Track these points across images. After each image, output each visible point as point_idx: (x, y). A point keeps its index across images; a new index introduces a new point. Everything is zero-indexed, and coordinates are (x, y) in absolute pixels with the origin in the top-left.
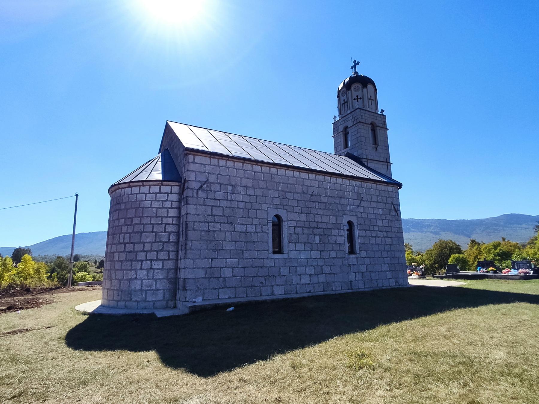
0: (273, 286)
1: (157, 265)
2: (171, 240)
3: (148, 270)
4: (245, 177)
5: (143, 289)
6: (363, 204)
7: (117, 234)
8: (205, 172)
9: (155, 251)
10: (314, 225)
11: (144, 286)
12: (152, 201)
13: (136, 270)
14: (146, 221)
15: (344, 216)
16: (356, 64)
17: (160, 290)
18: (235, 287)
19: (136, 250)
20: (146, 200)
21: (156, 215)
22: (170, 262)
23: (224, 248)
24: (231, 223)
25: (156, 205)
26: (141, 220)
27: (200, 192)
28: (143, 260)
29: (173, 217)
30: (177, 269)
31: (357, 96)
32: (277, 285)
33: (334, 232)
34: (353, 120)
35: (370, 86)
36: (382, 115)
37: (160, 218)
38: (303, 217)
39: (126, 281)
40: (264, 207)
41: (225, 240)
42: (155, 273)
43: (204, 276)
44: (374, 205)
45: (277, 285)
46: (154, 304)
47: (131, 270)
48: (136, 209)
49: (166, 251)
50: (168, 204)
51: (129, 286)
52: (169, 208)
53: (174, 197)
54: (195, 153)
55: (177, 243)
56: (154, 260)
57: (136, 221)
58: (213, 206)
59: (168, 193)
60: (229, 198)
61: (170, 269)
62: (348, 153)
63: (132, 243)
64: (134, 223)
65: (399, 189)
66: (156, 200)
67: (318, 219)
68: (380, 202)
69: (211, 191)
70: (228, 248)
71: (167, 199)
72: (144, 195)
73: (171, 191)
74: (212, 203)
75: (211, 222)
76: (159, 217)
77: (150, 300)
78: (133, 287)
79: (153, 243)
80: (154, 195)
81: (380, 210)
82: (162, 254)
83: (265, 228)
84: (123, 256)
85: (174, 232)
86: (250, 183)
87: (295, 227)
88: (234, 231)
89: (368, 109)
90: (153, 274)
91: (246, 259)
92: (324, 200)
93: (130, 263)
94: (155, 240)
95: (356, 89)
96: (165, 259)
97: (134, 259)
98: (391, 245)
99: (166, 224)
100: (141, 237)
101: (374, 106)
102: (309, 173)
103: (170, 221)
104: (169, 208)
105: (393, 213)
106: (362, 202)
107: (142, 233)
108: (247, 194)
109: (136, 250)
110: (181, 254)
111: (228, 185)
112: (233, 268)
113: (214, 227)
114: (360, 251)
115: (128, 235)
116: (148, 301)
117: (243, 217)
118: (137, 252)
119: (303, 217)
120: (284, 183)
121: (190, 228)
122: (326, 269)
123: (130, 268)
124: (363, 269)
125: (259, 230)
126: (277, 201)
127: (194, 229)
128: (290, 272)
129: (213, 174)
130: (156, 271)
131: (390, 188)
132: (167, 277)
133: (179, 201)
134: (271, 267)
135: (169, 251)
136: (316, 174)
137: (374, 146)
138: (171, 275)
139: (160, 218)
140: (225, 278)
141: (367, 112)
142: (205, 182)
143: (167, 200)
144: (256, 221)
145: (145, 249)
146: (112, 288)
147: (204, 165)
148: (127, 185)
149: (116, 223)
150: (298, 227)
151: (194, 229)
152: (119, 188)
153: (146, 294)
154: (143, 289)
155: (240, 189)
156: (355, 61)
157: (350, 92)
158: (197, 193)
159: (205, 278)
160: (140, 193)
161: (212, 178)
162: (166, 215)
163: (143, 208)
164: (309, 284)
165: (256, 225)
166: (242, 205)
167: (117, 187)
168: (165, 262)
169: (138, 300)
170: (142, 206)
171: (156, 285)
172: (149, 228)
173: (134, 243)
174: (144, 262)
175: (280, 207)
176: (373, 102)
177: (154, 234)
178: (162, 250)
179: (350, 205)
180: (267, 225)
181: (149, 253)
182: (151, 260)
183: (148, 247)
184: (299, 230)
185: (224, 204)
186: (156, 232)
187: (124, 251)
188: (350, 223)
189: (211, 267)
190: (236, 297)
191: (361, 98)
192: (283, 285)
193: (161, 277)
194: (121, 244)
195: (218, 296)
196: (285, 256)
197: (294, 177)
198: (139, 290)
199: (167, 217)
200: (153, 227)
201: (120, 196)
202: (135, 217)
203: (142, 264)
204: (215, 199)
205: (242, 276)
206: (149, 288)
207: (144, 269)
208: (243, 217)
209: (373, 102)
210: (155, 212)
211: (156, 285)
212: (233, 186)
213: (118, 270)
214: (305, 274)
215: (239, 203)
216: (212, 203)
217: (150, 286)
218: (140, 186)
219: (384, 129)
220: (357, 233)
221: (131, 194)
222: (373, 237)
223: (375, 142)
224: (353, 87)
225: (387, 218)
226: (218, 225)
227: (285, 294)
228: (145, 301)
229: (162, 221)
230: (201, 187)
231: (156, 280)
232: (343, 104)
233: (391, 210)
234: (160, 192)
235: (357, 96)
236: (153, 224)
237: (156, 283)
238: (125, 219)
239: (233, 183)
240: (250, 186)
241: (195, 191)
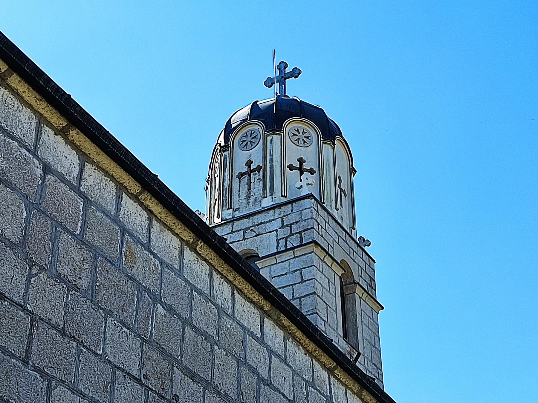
16: (285, 74)
31: (301, 161)
34: (282, 233)
156: (282, 66)
232: (241, 175)
235: (301, 161)
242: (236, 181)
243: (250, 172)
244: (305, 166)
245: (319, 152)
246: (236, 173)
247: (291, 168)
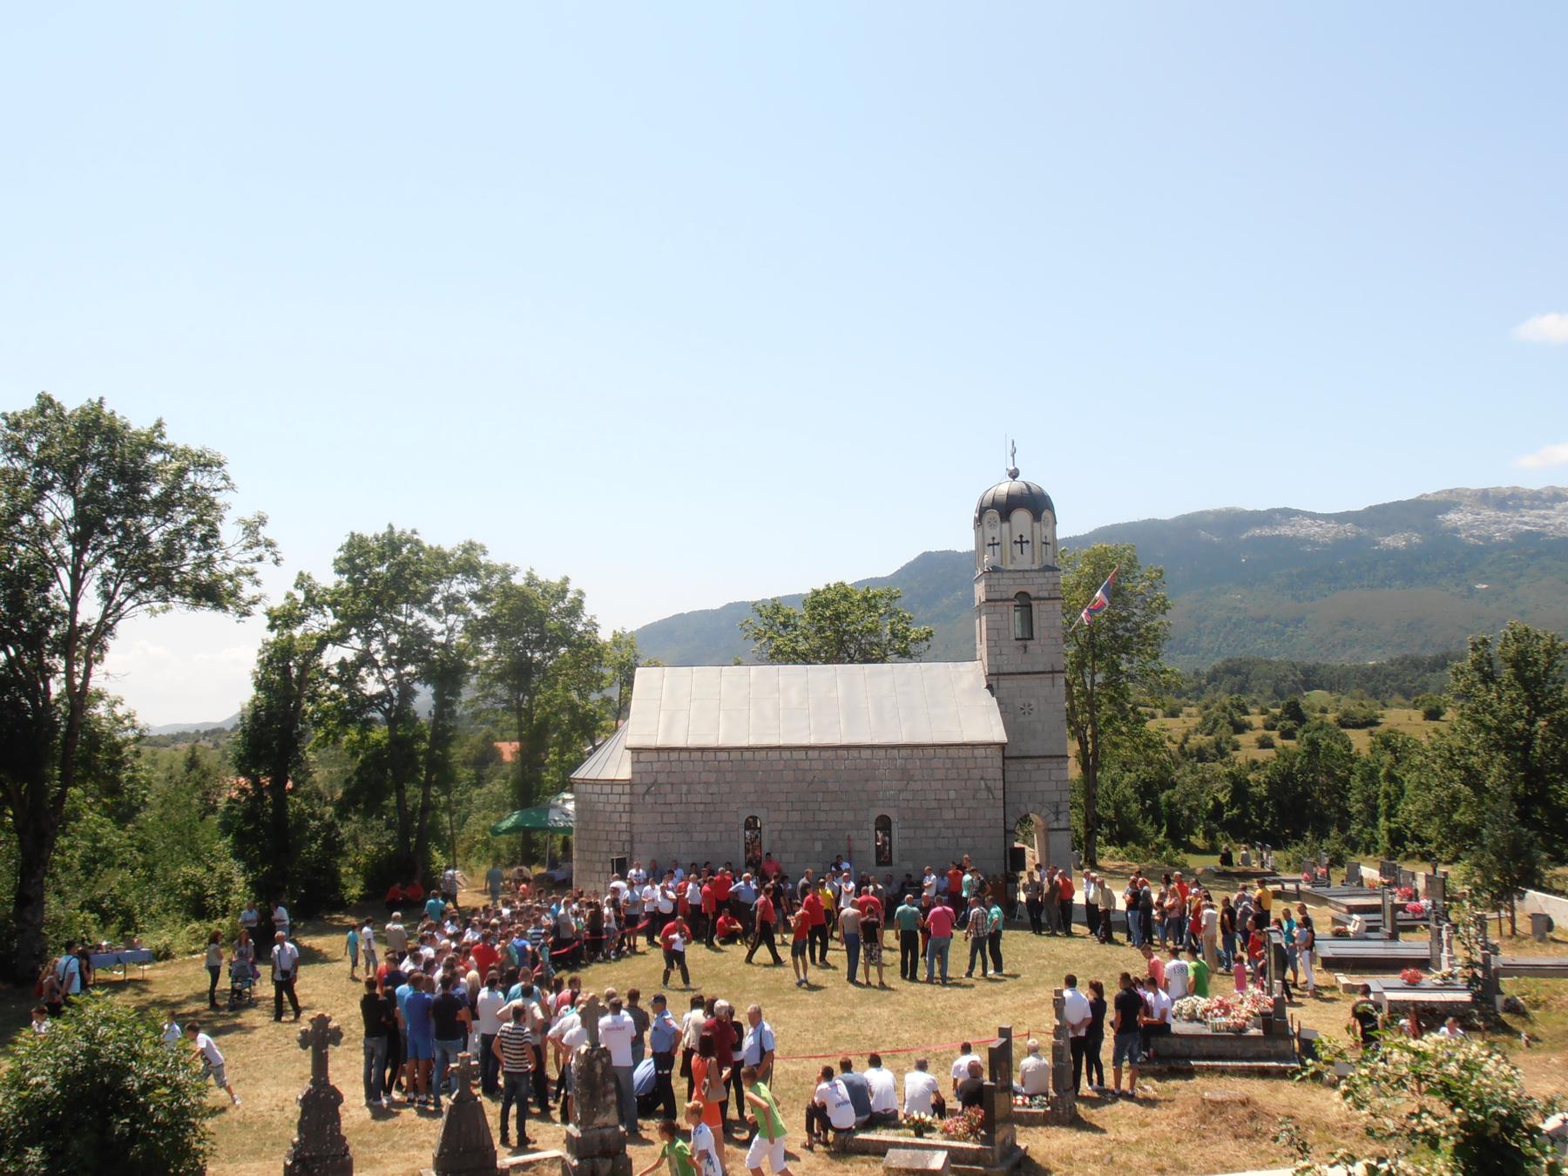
6: (912, 786)
14: (601, 827)
25: (609, 808)
38: (795, 816)
40: (733, 807)
44: (938, 785)
50: (620, 808)
57: (592, 826)
67: (822, 817)
74: (662, 808)
86: (713, 777)
89: (1011, 567)
92: (832, 787)
95: (991, 525)
103: (623, 827)
105: (984, 795)
126: (753, 798)
144: (721, 827)
155: (699, 788)
161: (662, 778)
166: (701, 808)
216: (662, 808)
224: (986, 519)
233: (976, 791)
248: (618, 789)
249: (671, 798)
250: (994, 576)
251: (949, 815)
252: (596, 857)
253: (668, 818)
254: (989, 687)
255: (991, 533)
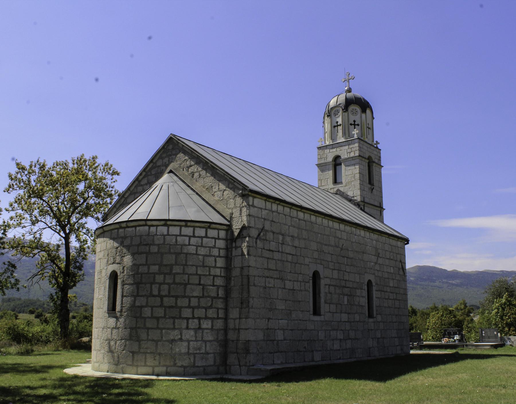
0: (312, 351)
1: (206, 324)
2: (220, 296)
3: (196, 330)
4: (292, 226)
5: (190, 352)
6: (380, 261)
7: (145, 284)
8: (262, 218)
9: (204, 307)
10: (343, 283)
11: (191, 348)
12: (197, 247)
13: (180, 329)
14: (192, 270)
15: (366, 274)
17: (211, 353)
18: (285, 352)
19: (179, 304)
20: (189, 245)
21: (203, 263)
22: (219, 321)
23: (277, 307)
24: (282, 279)
25: (202, 251)
26: (184, 269)
27: (258, 241)
28: (189, 318)
29: (221, 268)
30: (226, 330)
31: (354, 121)
32: (317, 351)
33: (358, 292)
35: (368, 111)
36: (377, 148)
37: (208, 268)
38: (335, 274)
39: (167, 343)
40: (307, 261)
41: (278, 299)
42: (205, 334)
43: (263, 338)
45: (317, 351)
46: (204, 369)
47: (174, 329)
48: (177, 254)
49: (215, 308)
50: (215, 252)
51: (171, 348)
52: (217, 257)
53: (221, 244)
54: (255, 195)
55: (226, 299)
56: (202, 318)
57: (177, 269)
58: (268, 258)
59: (215, 239)
60: (280, 249)
61: (220, 330)
62: (338, 190)
63: (173, 296)
64: (174, 271)
65: (406, 244)
66: (202, 246)
67: (346, 278)
68: (392, 259)
69: (267, 240)
70: (280, 308)
71: (215, 246)
72: (187, 238)
73: (218, 236)
74: (267, 254)
75: (268, 277)
76: (207, 266)
77: (199, 365)
78: (177, 350)
79: (201, 297)
80: (199, 240)
81: (392, 268)
82: (211, 312)
83: (307, 284)
84: (160, 312)
85: (223, 286)
86: (294, 232)
87: (329, 285)
88: (284, 288)
89: (366, 140)
90: (202, 335)
91: (294, 320)
92: (351, 255)
93: (172, 320)
94: (203, 294)
95: (355, 113)
96: (214, 318)
97: (178, 317)
98: (399, 308)
99: (214, 276)
100: (185, 289)
101: (370, 136)
102: (340, 223)
103: (218, 272)
104: (217, 257)
105: (401, 273)
106: (379, 259)
107: (186, 285)
108: (293, 246)
109: (179, 304)
110: (234, 313)
111: (277, 234)
112: (284, 330)
113: (269, 283)
114: (377, 314)
115: (166, 287)
116: (198, 367)
117: (290, 272)
118: (181, 307)
119: (335, 274)
120: (321, 234)
121: (251, 283)
122: (352, 334)
123: (172, 326)
124: (379, 335)
125: (303, 288)
126: (316, 255)
127: (254, 285)
128: (325, 337)
129: (268, 220)
130: (205, 331)
131: (399, 244)
132: (217, 339)
133: (228, 249)
134: (312, 330)
135: (218, 309)
136: (345, 225)
137: (370, 186)
138: (221, 337)
139: (208, 268)
140: (278, 341)
141: (365, 144)
142: (262, 229)
143: (214, 247)
144: (300, 278)
145: (191, 305)
146: (142, 350)
147: (261, 209)
148: (162, 223)
149: (143, 269)
150: (332, 285)
151: (254, 285)
152: (146, 225)
153: (195, 357)
154: (190, 352)
155: (288, 239)
157: (346, 114)
158: (256, 243)
159: (264, 340)
160: (180, 235)
161: (267, 226)
162: (214, 265)
163: (187, 254)
164: (339, 350)
165: (301, 282)
166: (290, 258)
167: (144, 223)
168: (215, 321)
169: (184, 365)
170: (185, 251)
171: (206, 348)
172: (195, 280)
173: (177, 297)
174: (190, 321)
175: (319, 261)
176: (370, 131)
177: (201, 287)
178: (211, 307)
179: (370, 262)
180: (309, 282)
181: (196, 310)
182: (199, 319)
183: (194, 302)
184: (332, 289)
185: (277, 256)
186: (204, 285)
187: (161, 306)
188: (369, 283)
189: (268, 329)
190: (286, 363)
191: (358, 125)
192: (320, 351)
193: (211, 338)
194: (154, 296)
195: (274, 361)
196: (322, 318)
197: (328, 227)
198: (185, 354)
199: (215, 267)
200: (200, 278)
201: (148, 235)
202: (176, 264)
203: (188, 323)
204: (270, 250)
205: (290, 340)
206: (198, 351)
207: (191, 329)
208: (290, 272)
209: (370, 131)
210: (202, 260)
211: (206, 348)
212: (283, 235)
213: (152, 328)
214: (336, 339)
215: (288, 255)
217: (199, 349)
218: (181, 226)
219: (379, 166)
220: (375, 294)
221: (168, 235)
222: (385, 299)
223: (371, 182)
225: (397, 278)
226: (272, 281)
227: (322, 360)
228: (194, 366)
229: (210, 271)
230: (259, 234)
231: (206, 342)
234: (206, 236)
235: (354, 121)
236: (200, 275)
237: (206, 346)
238: (161, 265)
239: (283, 232)
240: (296, 235)
241: (255, 240)
242: (333, 128)
243: (338, 126)
244: (356, 123)
245: (361, 117)
246: (333, 126)
247: (351, 124)
248: (212, 233)
249: (273, 246)
250: (362, 142)
251: (391, 285)
252: (184, 302)
253: (272, 266)
254: (361, 209)
255: (352, 118)
